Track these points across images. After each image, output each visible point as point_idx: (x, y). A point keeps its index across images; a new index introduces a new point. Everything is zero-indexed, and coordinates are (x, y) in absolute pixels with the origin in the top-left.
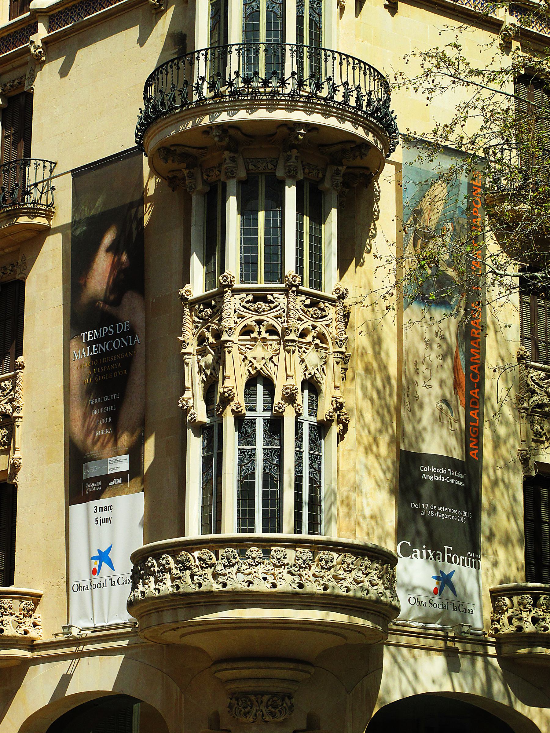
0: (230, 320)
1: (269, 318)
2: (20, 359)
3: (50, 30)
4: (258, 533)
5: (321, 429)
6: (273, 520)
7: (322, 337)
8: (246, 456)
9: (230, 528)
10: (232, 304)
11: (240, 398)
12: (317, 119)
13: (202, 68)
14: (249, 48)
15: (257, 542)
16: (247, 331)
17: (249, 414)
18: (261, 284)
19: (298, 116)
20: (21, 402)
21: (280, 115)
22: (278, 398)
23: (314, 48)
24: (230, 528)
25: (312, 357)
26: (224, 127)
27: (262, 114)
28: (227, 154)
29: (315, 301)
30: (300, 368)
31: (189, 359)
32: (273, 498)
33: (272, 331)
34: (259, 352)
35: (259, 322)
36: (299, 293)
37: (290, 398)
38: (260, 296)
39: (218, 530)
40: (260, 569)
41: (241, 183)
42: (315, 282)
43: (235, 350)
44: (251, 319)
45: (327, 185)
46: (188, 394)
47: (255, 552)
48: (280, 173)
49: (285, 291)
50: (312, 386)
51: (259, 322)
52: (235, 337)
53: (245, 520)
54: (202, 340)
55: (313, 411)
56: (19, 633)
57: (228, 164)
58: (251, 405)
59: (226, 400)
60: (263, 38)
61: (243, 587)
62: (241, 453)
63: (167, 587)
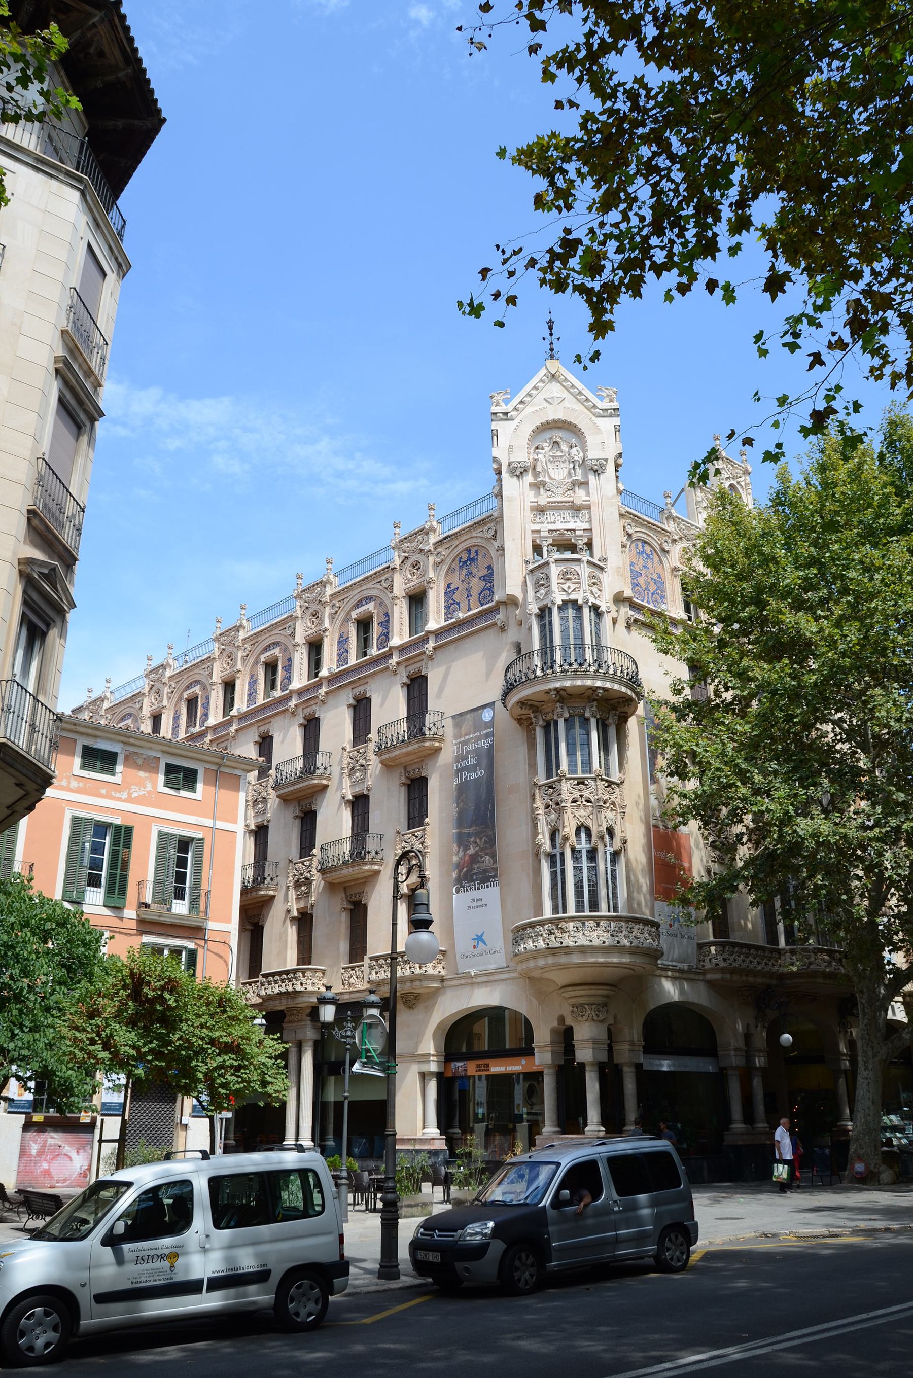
0: (565, 795)
1: (586, 794)
2: (427, 820)
3: (436, 641)
4: (587, 913)
5: (615, 855)
6: (594, 906)
7: (613, 804)
8: (578, 870)
9: (572, 911)
10: (565, 786)
11: (573, 838)
12: (608, 685)
13: (537, 661)
14: (565, 647)
15: (573, 919)
16: (574, 801)
17: (578, 847)
18: (580, 775)
19: (599, 684)
20: (428, 843)
21: (589, 683)
22: (594, 838)
23: (598, 648)
24: (572, 911)
25: (610, 815)
26: (558, 691)
27: (579, 683)
28: (558, 705)
29: (610, 784)
30: (604, 821)
31: (540, 817)
32: (594, 893)
33: (588, 801)
34: (582, 812)
35: (581, 796)
36: (602, 780)
37: (602, 838)
38: (581, 782)
39: (565, 911)
40: (595, 934)
41: (566, 720)
42: (607, 775)
43: (569, 811)
44: (577, 795)
45: (610, 721)
46: (540, 836)
47: (592, 923)
48: (587, 715)
49: (594, 779)
50: (610, 831)
51: (581, 796)
52: (569, 804)
53: (579, 906)
54: (547, 807)
55: (612, 845)
56: (435, 972)
57: (559, 710)
58: (579, 842)
59: (566, 839)
60: (572, 642)
61: (587, 943)
62: (575, 868)
63: (541, 944)
